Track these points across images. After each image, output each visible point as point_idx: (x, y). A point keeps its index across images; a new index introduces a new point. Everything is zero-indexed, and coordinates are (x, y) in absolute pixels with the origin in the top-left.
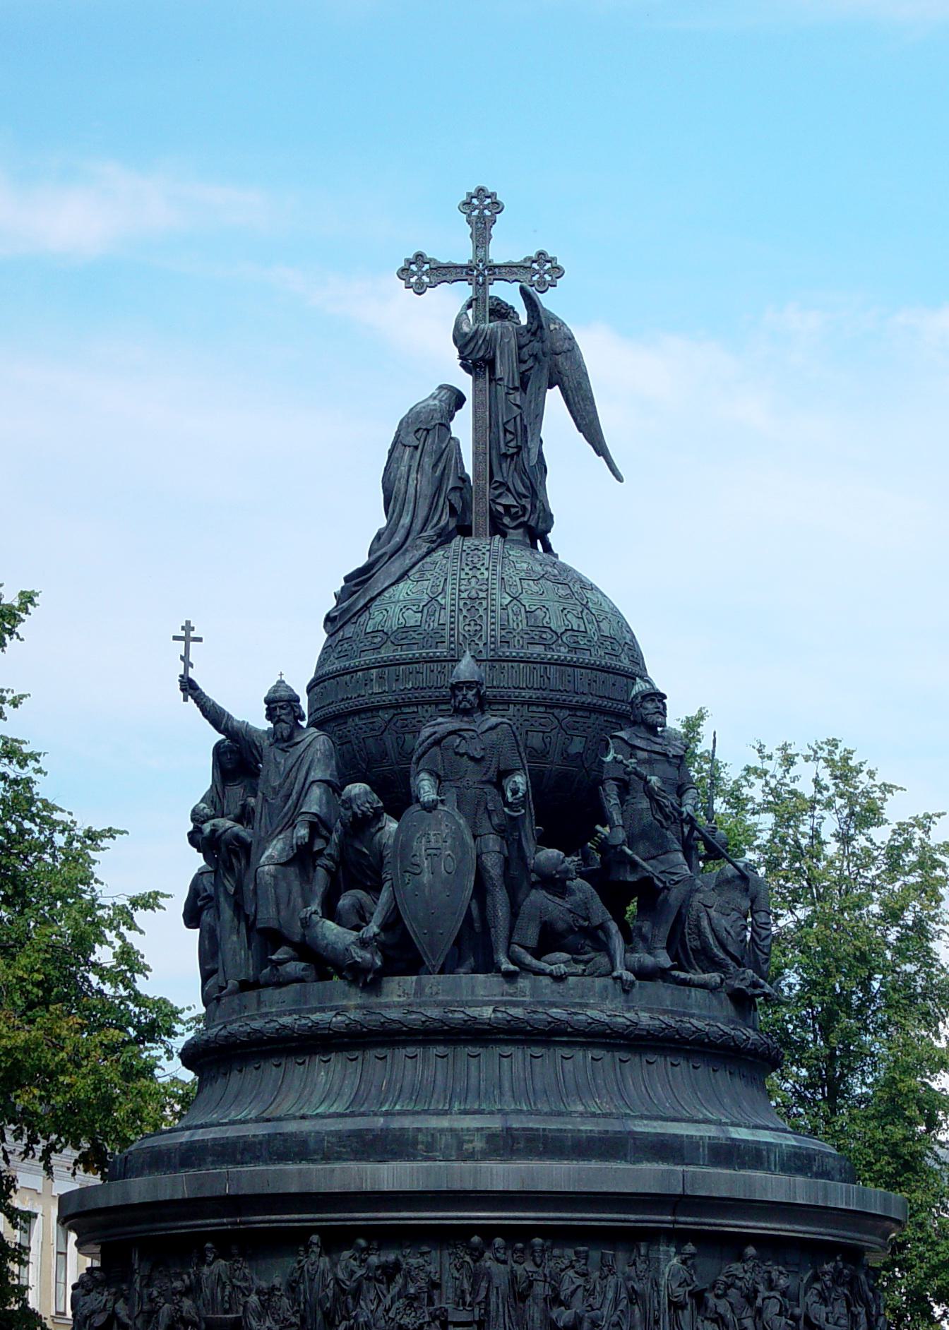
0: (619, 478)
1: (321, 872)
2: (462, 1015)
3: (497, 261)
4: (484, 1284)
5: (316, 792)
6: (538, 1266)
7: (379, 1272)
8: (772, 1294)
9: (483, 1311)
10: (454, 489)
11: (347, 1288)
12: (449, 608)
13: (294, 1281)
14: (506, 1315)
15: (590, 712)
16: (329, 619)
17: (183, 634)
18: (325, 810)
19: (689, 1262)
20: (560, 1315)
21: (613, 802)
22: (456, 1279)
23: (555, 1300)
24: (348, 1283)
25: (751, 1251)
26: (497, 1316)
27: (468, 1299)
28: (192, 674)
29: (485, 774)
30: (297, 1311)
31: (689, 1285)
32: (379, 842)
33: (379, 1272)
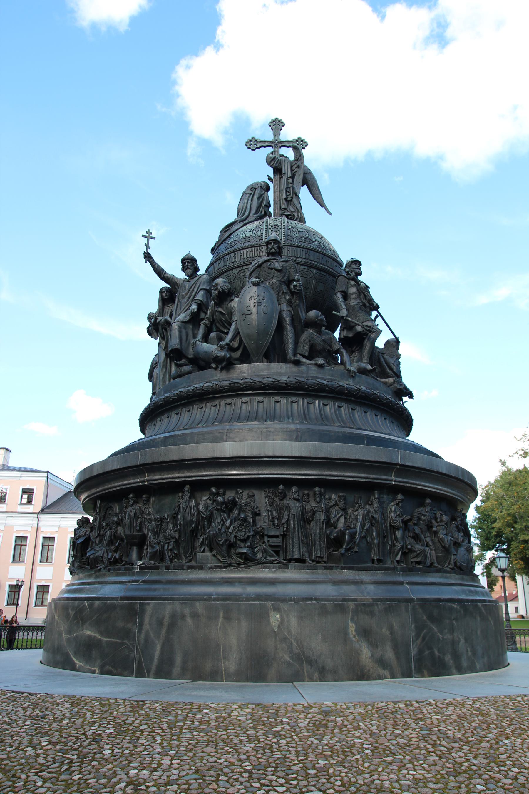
0: (331, 214)
1: (202, 327)
2: (270, 379)
3: (282, 140)
4: (286, 513)
5: (202, 293)
6: (318, 503)
7: (224, 506)
8: (441, 524)
9: (285, 529)
10: (265, 205)
11: (204, 516)
12: (264, 229)
13: (175, 513)
14: (300, 531)
15: (327, 273)
16: (213, 250)
17: (147, 235)
18: (205, 300)
19: (400, 505)
20: (331, 533)
21: (341, 300)
22: (269, 511)
23: (328, 523)
24: (205, 513)
25: (428, 501)
26: (294, 531)
27: (276, 522)
28: (149, 251)
29: (282, 278)
30: (176, 531)
31: (401, 517)
32: (231, 306)
33: (224, 506)
